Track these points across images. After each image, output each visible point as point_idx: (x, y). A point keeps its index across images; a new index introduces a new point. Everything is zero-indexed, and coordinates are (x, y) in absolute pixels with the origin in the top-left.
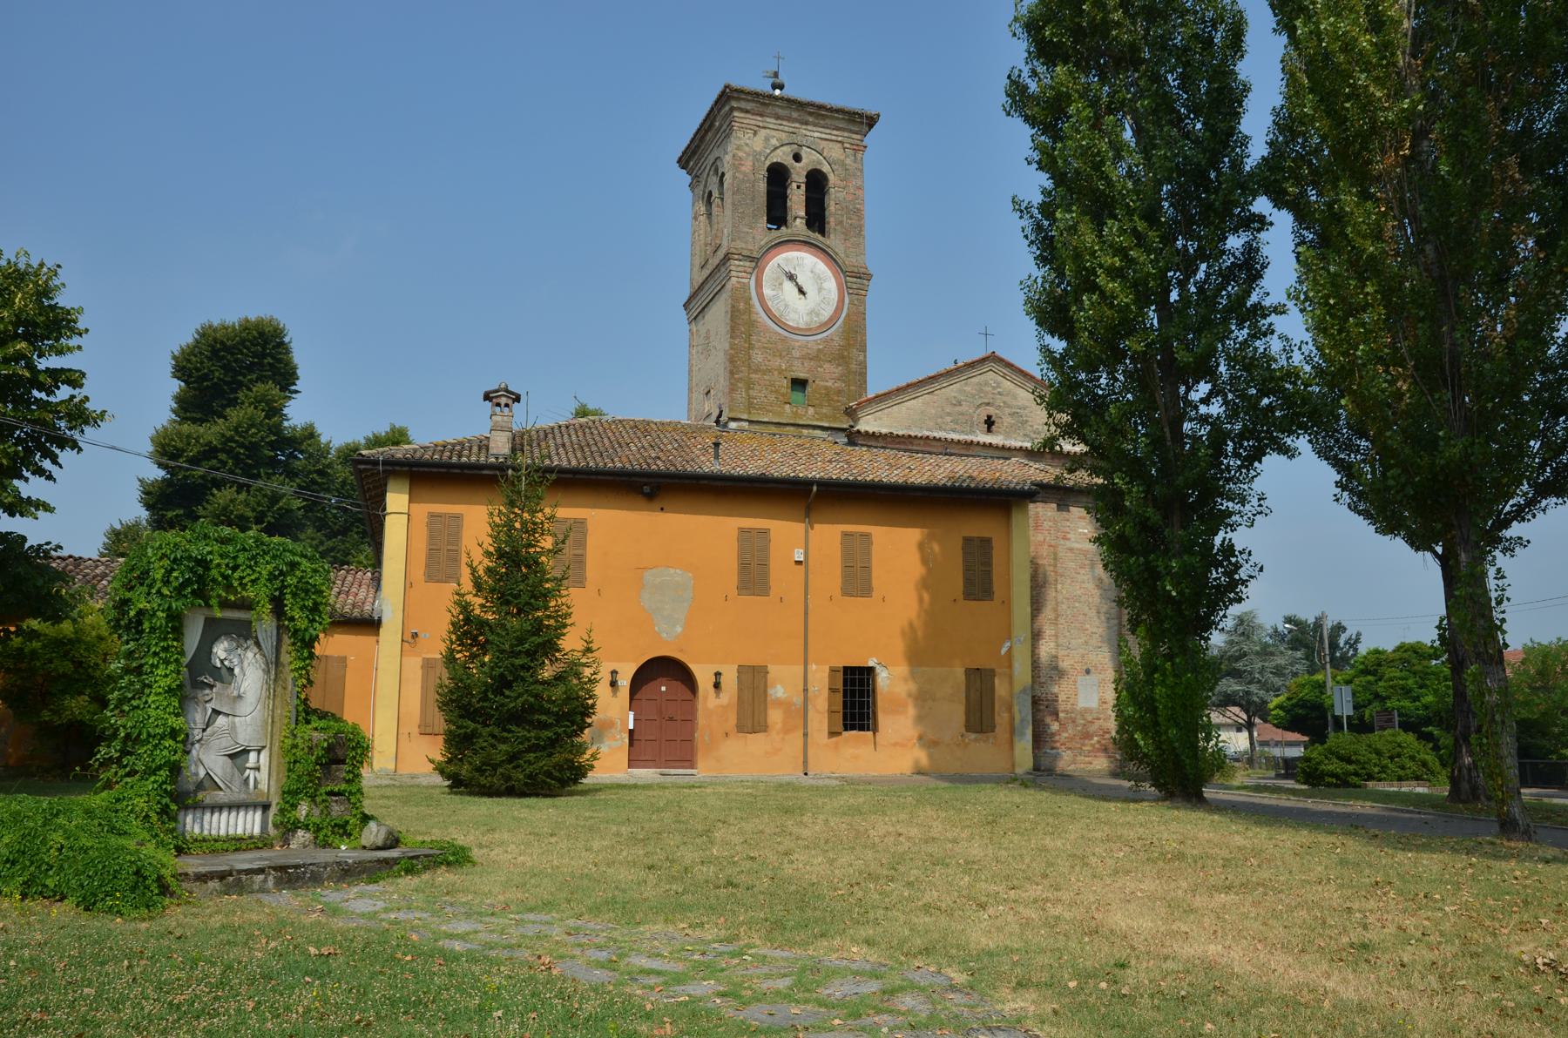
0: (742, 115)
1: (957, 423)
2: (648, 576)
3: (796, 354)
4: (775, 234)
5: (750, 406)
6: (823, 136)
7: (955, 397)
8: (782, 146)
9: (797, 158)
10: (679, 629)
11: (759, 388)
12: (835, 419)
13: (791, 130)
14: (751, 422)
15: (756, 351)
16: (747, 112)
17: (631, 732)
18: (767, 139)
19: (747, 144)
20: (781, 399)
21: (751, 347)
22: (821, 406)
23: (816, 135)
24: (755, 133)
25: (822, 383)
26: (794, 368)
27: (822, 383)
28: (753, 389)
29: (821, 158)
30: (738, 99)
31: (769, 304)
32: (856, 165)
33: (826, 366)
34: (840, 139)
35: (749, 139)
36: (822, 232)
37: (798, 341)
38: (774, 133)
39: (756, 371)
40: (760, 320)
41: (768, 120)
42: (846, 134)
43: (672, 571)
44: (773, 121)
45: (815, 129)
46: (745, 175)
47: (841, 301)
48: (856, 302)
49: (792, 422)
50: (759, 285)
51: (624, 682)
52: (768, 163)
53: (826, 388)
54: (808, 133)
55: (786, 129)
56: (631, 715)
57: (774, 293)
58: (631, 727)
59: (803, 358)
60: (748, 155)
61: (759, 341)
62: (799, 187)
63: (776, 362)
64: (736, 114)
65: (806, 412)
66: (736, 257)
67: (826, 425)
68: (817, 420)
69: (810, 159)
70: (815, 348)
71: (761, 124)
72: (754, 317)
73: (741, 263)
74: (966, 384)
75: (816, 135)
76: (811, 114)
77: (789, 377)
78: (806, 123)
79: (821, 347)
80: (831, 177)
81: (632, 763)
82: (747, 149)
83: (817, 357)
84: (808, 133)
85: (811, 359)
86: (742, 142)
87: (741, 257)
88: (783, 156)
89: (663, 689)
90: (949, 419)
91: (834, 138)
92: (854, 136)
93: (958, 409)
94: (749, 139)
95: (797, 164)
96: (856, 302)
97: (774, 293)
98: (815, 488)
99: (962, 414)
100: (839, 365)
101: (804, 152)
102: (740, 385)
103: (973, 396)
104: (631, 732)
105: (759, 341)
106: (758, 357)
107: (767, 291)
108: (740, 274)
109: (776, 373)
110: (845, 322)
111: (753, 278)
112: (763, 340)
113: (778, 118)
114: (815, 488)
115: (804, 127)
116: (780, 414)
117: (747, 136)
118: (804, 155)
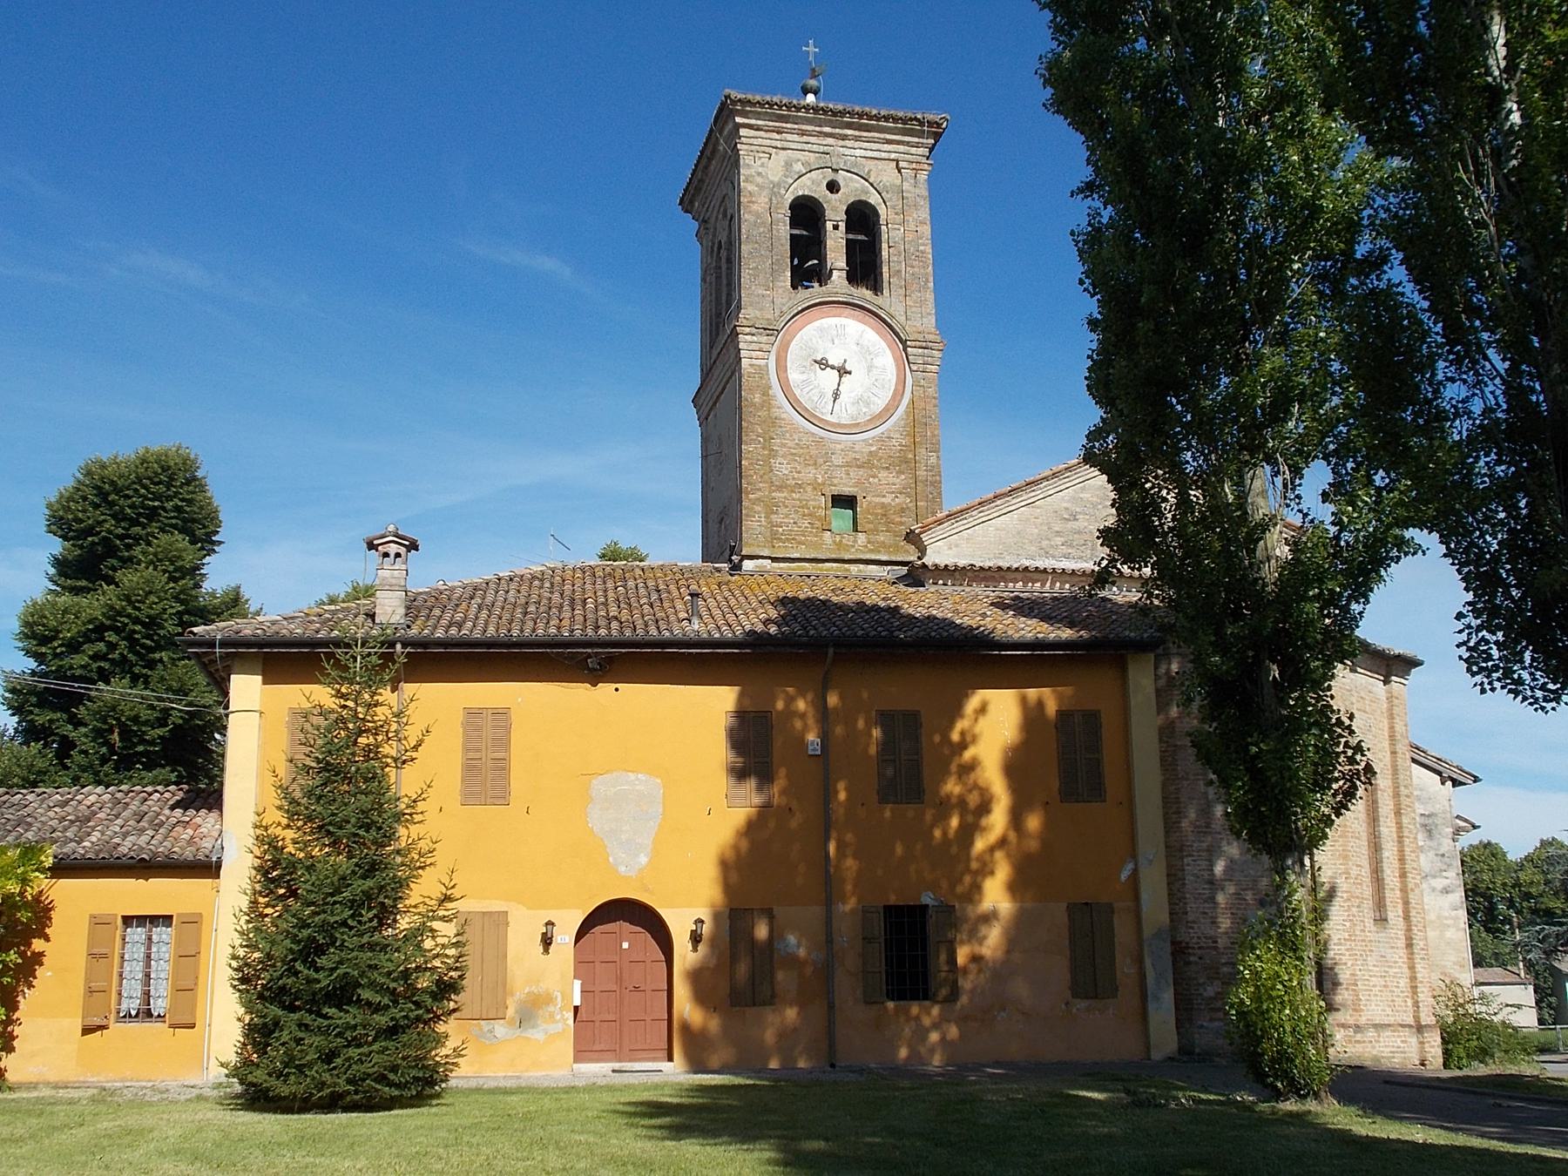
0: (752, 133)
1: (1071, 546)
2: (599, 786)
3: (837, 460)
4: (802, 293)
5: (774, 537)
6: (870, 154)
7: (1067, 509)
8: (810, 171)
9: (833, 187)
10: (643, 859)
12: (897, 549)
13: (822, 149)
14: (774, 560)
15: (780, 460)
16: (758, 129)
17: (576, 1008)
19: (759, 174)
20: (818, 524)
21: (773, 454)
22: (876, 531)
23: (858, 152)
25: (877, 500)
26: (835, 481)
27: (877, 500)
28: (776, 513)
29: (867, 184)
30: (745, 114)
31: (797, 392)
34: (893, 156)
35: (762, 165)
36: (876, 288)
38: (798, 155)
39: (780, 488)
40: (784, 416)
41: (789, 137)
42: (901, 148)
43: (632, 776)
44: (796, 138)
45: (857, 144)
46: (758, 215)
47: (902, 381)
49: (834, 556)
51: (565, 937)
52: (789, 197)
53: (883, 506)
54: (847, 152)
55: (815, 148)
56: (577, 984)
57: (804, 377)
58: (577, 1002)
59: (848, 465)
60: (761, 187)
61: (784, 445)
62: (836, 227)
63: (810, 474)
64: (743, 132)
65: (855, 541)
66: (747, 330)
67: (884, 558)
68: (871, 551)
69: (852, 188)
70: (866, 450)
71: (779, 144)
72: (776, 412)
73: (755, 338)
74: (1083, 489)
75: (858, 152)
76: (849, 126)
77: (829, 494)
78: (844, 138)
79: (874, 449)
80: (882, 210)
81: (581, 1054)
82: (759, 180)
83: (867, 464)
84: (847, 152)
85: (859, 467)
86: (752, 171)
87: (754, 330)
88: (813, 186)
89: (625, 945)
90: (1059, 540)
91: (884, 155)
92: (913, 150)
93: (1072, 525)
94: (762, 165)
95: (834, 196)
97: (804, 377)
99: (1079, 532)
100: (900, 472)
101: (841, 177)
102: (757, 508)
103: (1094, 506)
104: (576, 1008)
105: (784, 445)
106: (782, 468)
107: (794, 376)
108: (754, 354)
109: (809, 489)
111: (773, 358)
112: (790, 444)
113: (803, 133)
115: (841, 143)
116: (817, 546)
117: (759, 163)
118: (842, 184)
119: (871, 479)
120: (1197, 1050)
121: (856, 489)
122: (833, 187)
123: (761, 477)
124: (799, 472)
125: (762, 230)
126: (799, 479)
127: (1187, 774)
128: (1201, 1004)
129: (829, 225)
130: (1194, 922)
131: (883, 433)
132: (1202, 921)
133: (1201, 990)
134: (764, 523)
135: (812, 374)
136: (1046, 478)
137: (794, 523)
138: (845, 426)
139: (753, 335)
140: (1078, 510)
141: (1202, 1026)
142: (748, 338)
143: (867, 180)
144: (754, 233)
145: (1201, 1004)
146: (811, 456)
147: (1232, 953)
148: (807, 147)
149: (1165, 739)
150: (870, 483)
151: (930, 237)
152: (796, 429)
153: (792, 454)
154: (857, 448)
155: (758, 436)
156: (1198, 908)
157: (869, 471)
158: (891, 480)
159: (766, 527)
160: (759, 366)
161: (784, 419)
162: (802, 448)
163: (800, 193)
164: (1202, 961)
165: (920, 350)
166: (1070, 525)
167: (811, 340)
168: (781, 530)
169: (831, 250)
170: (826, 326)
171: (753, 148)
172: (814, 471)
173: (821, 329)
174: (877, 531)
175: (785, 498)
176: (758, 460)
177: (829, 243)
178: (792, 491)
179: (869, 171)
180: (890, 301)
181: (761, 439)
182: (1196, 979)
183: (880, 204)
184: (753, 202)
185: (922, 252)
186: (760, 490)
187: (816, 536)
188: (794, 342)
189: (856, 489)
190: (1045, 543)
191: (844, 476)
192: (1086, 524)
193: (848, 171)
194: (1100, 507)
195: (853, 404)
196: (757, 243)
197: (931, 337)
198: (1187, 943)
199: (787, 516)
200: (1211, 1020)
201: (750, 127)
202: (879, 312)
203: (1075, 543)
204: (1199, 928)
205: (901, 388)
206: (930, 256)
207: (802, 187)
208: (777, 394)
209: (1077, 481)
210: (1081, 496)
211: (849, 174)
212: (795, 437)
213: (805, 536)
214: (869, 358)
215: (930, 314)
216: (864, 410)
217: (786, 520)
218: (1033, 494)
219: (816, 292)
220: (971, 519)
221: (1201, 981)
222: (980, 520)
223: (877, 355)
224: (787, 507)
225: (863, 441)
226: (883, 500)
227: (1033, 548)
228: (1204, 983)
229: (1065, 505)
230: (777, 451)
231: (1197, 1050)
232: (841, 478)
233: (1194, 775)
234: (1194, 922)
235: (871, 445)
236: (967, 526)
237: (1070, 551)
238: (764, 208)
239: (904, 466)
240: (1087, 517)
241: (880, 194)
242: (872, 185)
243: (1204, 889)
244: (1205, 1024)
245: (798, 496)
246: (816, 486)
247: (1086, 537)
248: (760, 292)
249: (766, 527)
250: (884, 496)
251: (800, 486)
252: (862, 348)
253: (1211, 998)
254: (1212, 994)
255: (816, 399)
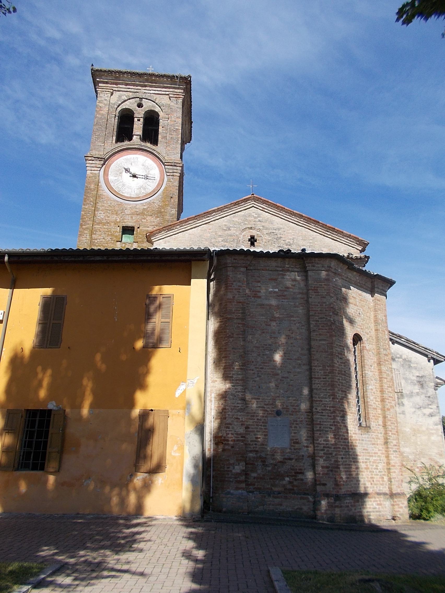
1: (227, 242)
4: (119, 144)
7: (225, 225)
8: (130, 99)
11: (100, 233)
13: (135, 91)
15: (100, 212)
18: (120, 97)
20: (114, 239)
23: (152, 92)
24: (112, 94)
25: (145, 229)
26: (125, 221)
27: (145, 229)
28: (95, 234)
29: (155, 104)
31: (112, 184)
32: (177, 106)
33: (149, 218)
34: (167, 93)
37: (130, 205)
41: (121, 86)
44: (124, 86)
45: (151, 89)
46: (103, 115)
47: (162, 180)
48: (172, 180)
50: (106, 174)
55: (132, 90)
57: (116, 178)
59: (132, 214)
60: (106, 105)
62: (139, 120)
63: (113, 218)
66: (90, 158)
69: (148, 105)
70: (142, 208)
73: (94, 162)
74: (234, 216)
75: (152, 92)
79: (145, 207)
80: (161, 114)
83: (142, 213)
85: (138, 215)
86: (103, 99)
87: (93, 159)
88: (131, 105)
90: (220, 239)
92: (176, 90)
93: (229, 232)
96: (172, 180)
97: (116, 178)
98: (6, 258)
99: (231, 236)
100: (157, 217)
103: (240, 224)
105: (103, 206)
106: (100, 215)
107: (111, 178)
108: (93, 169)
109: (112, 224)
110: (163, 193)
112: (106, 205)
113: (127, 85)
114: (6, 258)
118: (144, 104)
119: (143, 220)
120: (224, 509)
121: (134, 224)
122: (140, 105)
123: (90, 219)
124: (109, 217)
125: (103, 120)
126: (108, 220)
127: (233, 334)
128: (230, 478)
129: (136, 120)
130: (230, 424)
131: (151, 201)
132: (236, 423)
133: (231, 468)
134: (88, 238)
135: (120, 177)
136: (214, 211)
137: (103, 238)
138: (133, 198)
139: (93, 160)
140: (231, 225)
141: (229, 493)
142: (91, 162)
143: (154, 102)
144: (100, 122)
145: (230, 478)
146: (115, 211)
147: (256, 444)
148: (128, 90)
149: (222, 315)
150: (142, 222)
151: (181, 123)
152: (109, 199)
153: (106, 209)
154: (138, 207)
155: (90, 202)
156: (233, 415)
157: (142, 217)
158: (152, 220)
159: (89, 240)
160: (95, 173)
161: (104, 195)
162: (111, 207)
163: (124, 108)
164: (233, 449)
165: (171, 167)
166: (226, 232)
167: (121, 163)
168: (96, 241)
169: (135, 129)
170: (129, 158)
171: (103, 90)
172: (116, 217)
173: (127, 159)
174: (143, 242)
175: (100, 228)
176: (89, 212)
177: (135, 126)
178: (104, 225)
179: (156, 99)
180: (160, 148)
181: (92, 203)
182: (228, 460)
183: (159, 111)
184: (101, 110)
185: (177, 129)
186: (88, 224)
187: (113, 244)
188: (113, 164)
189: (134, 224)
190: (213, 240)
191: (130, 218)
192: (235, 232)
193: (147, 99)
194: (242, 224)
195: (138, 189)
196: (100, 125)
197: (177, 162)
198: (225, 437)
199: (100, 235)
200: (237, 489)
201: (104, 83)
202: (153, 152)
203: (228, 241)
204: (233, 428)
205: (161, 183)
206: (181, 131)
207: (125, 105)
208: (103, 185)
209: (231, 213)
210: (233, 219)
211: (147, 100)
212: (109, 202)
213: (107, 244)
214: (148, 170)
215: (178, 153)
216: (143, 191)
217: (99, 237)
218: (208, 218)
219: (126, 144)
220: (176, 230)
221: (232, 462)
222: (181, 230)
223: (151, 169)
224: (101, 231)
225: (141, 204)
226: (148, 229)
227: (207, 243)
228: (234, 464)
229: (225, 223)
230: (99, 208)
231: (224, 509)
232: (129, 219)
233: (238, 335)
234: (230, 424)
235: (145, 206)
236: (174, 233)
237: (225, 244)
238: (106, 112)
239: (159, 214)
240: (236, 229)
241: (160, 107)
242: (157, 104)
243: (238, 403)
244: (232, 491)
245: (107, 227)
246: (116, 223)
247: (234, 238)
248: (99, 144)
249: (89, 240)
250: (148, 227)
251: (108, 223)
252: (145, 167)
253: (237, 474)
254: (239, 471)
255: (120, 187)
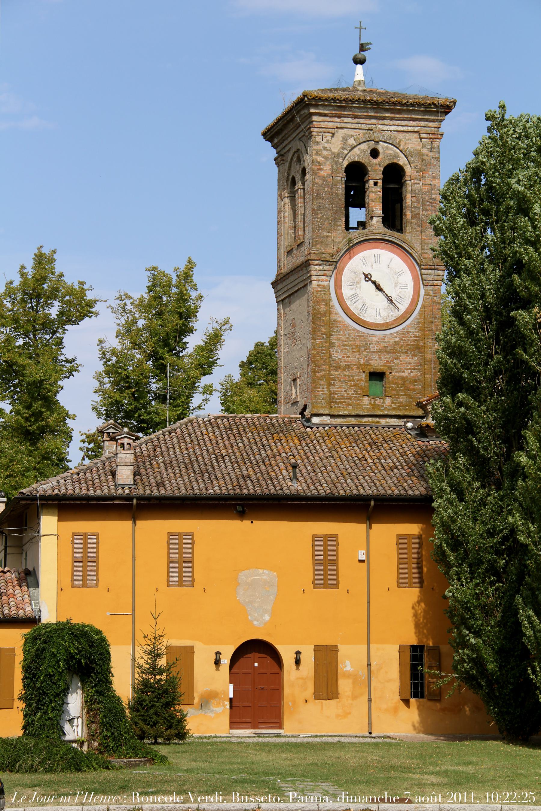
0: (321, 118)
2: (243, 576)
3: (374, 348)
5: (331, 400)
6: (400, 128)
8: (360, 144)
9: (375, 153)
10: (267, 618)
11: (339, 383)
12: (411, 409)
13: (368, 127)
14: (332, 416)
16: (325, 115)
17: (231, 699)
18: (345, 139)
19: (325, 148)
20: (360, 391)
21: (331, 345)
22: (398, 396)
24: (333, 135)
25: (399, 374)
28: (334, 385)
29: (398, 151)
30: (316, 106)
31: (348, 302)
32: (432, 154)
33: (403, 357)
34: (416, 129)
35: (327, 142)
36: (400, 230)
37: (375, 336)
38: (351, 132)
39: (337, 367)
40: (339, 319)
41: (346, 120)
42: (423, 123)
43: (261, 571)
44: (350, 120)
45: (392, 122)
48: (431, 293)
49: (370, 413)
50: (338, 286)
51: (226, 661)
52: (345, 163)
53: (403, 378)
54: (385, 128)
55: (363, 126)
56: (231, 686)
57: (353, 292)
58: (231, 696)
59: (380, 351)
60: (326, 158)
61: (339, 339)
62: (376, 184)
63: (355, 358)
64: (315, 118)
65: (384, 403)
66: (316, 262)
67: (402, 413)
68: (394, 409)
71: (339, 125)
72: (334, 317)
73: (321, 267)
76: (387, 110)
77: (367, 371)
78: (384, 118)
79: (397, 339)
80: (408, 170)
81: (233, 724)
82: (325, 153)
84: (385, 128)
85: (387, 352)
86: (320, 147)
87: (321, 262)
89: (256, 665)
91: (410, 129)
92: (431, 124)
94: (327, 142)
95: (374, 161)
96: (431, 293)
98: (372, 503)
100: (414, 355)
101: (381, 147)
102: (322, 382)
104: (231, 699)
105: (339, 339)
106: (338, 354)
107: (346, 292)
109: (354, 368)
110: (420, 314)
111: (333, 280)
112: (343, 338)
113: (355, 117)
114: (372, 503)
115: (381, 122)
116: (359, 406)
117: (325, 140)
118: (381, 151)
119: (395, 361)
122: (375, 153)
123: (324, 361)
125: (326, 189)
126: (348, 362)
131: (404, 329)
134: (325, 392)
137: (345, 391)
139: (320, 265)
142: (317, 267)
143: (398, 148)
150: (394, 363)
152: (346, 327)
154: (387, 339)
158: (408, 361)
160: (324, 286)
161: (339, 321)
162: (351, 341)
168: (336, 396)
171: (321, 130)
172: (358, 356)
175: (339, 375)
176: (322, 350)
178: (344, 370)
179: (400, 141)
183: (406, 165)
186: (323, 370)
187: (359, 400)
191: (378, 359)
193: (385, 142)
196: (323, 199)
202: (404, 245)
205: (416, 297)
211: (386, 144)
213: (350, 399)
217: (339, 390)
225: (391, 334)
230: (334, 343)
235: (396, 337)
239: (417, 351)
241: (406, 158)
242: (401, 151)
250: (403, 372)
251: (349, 366)
